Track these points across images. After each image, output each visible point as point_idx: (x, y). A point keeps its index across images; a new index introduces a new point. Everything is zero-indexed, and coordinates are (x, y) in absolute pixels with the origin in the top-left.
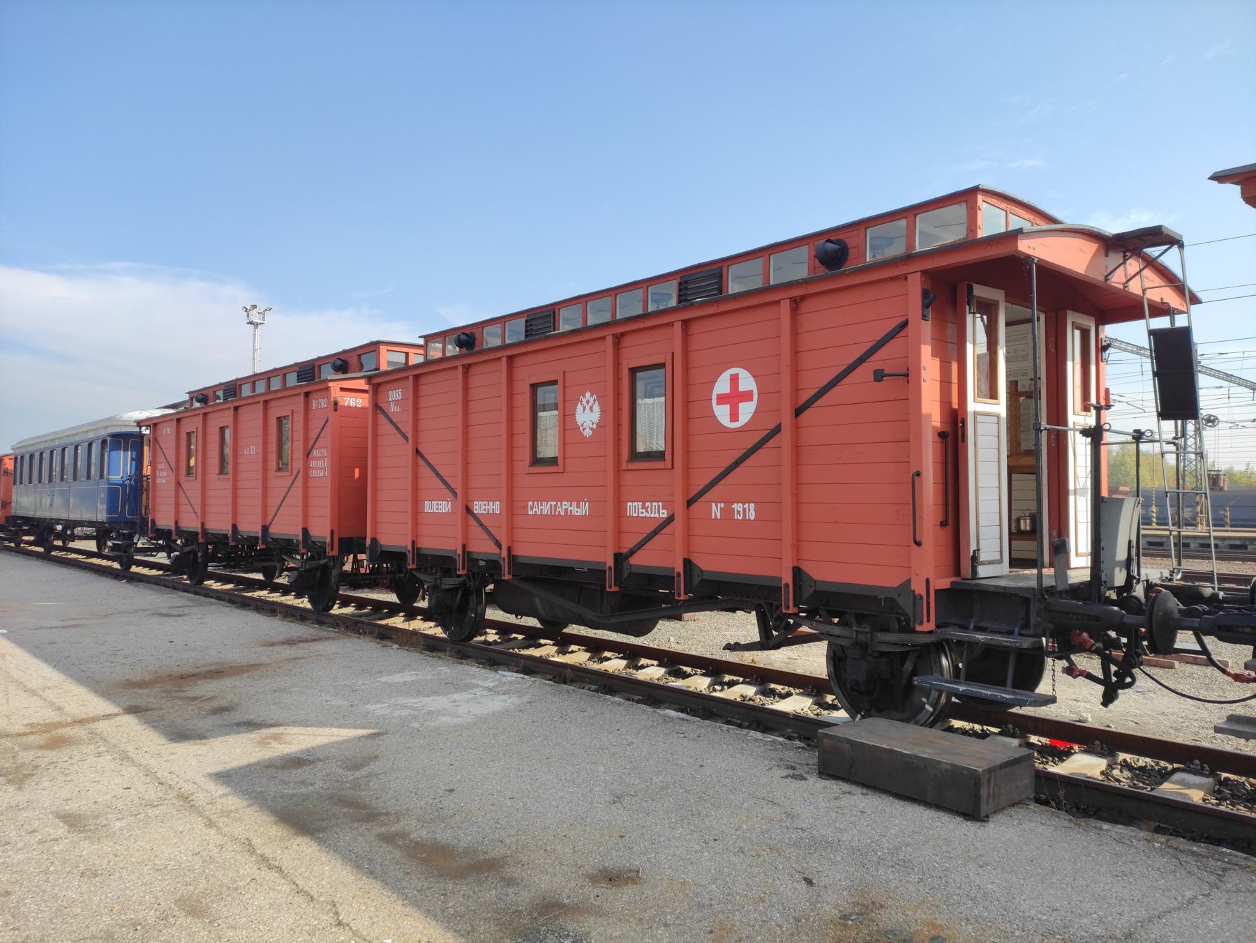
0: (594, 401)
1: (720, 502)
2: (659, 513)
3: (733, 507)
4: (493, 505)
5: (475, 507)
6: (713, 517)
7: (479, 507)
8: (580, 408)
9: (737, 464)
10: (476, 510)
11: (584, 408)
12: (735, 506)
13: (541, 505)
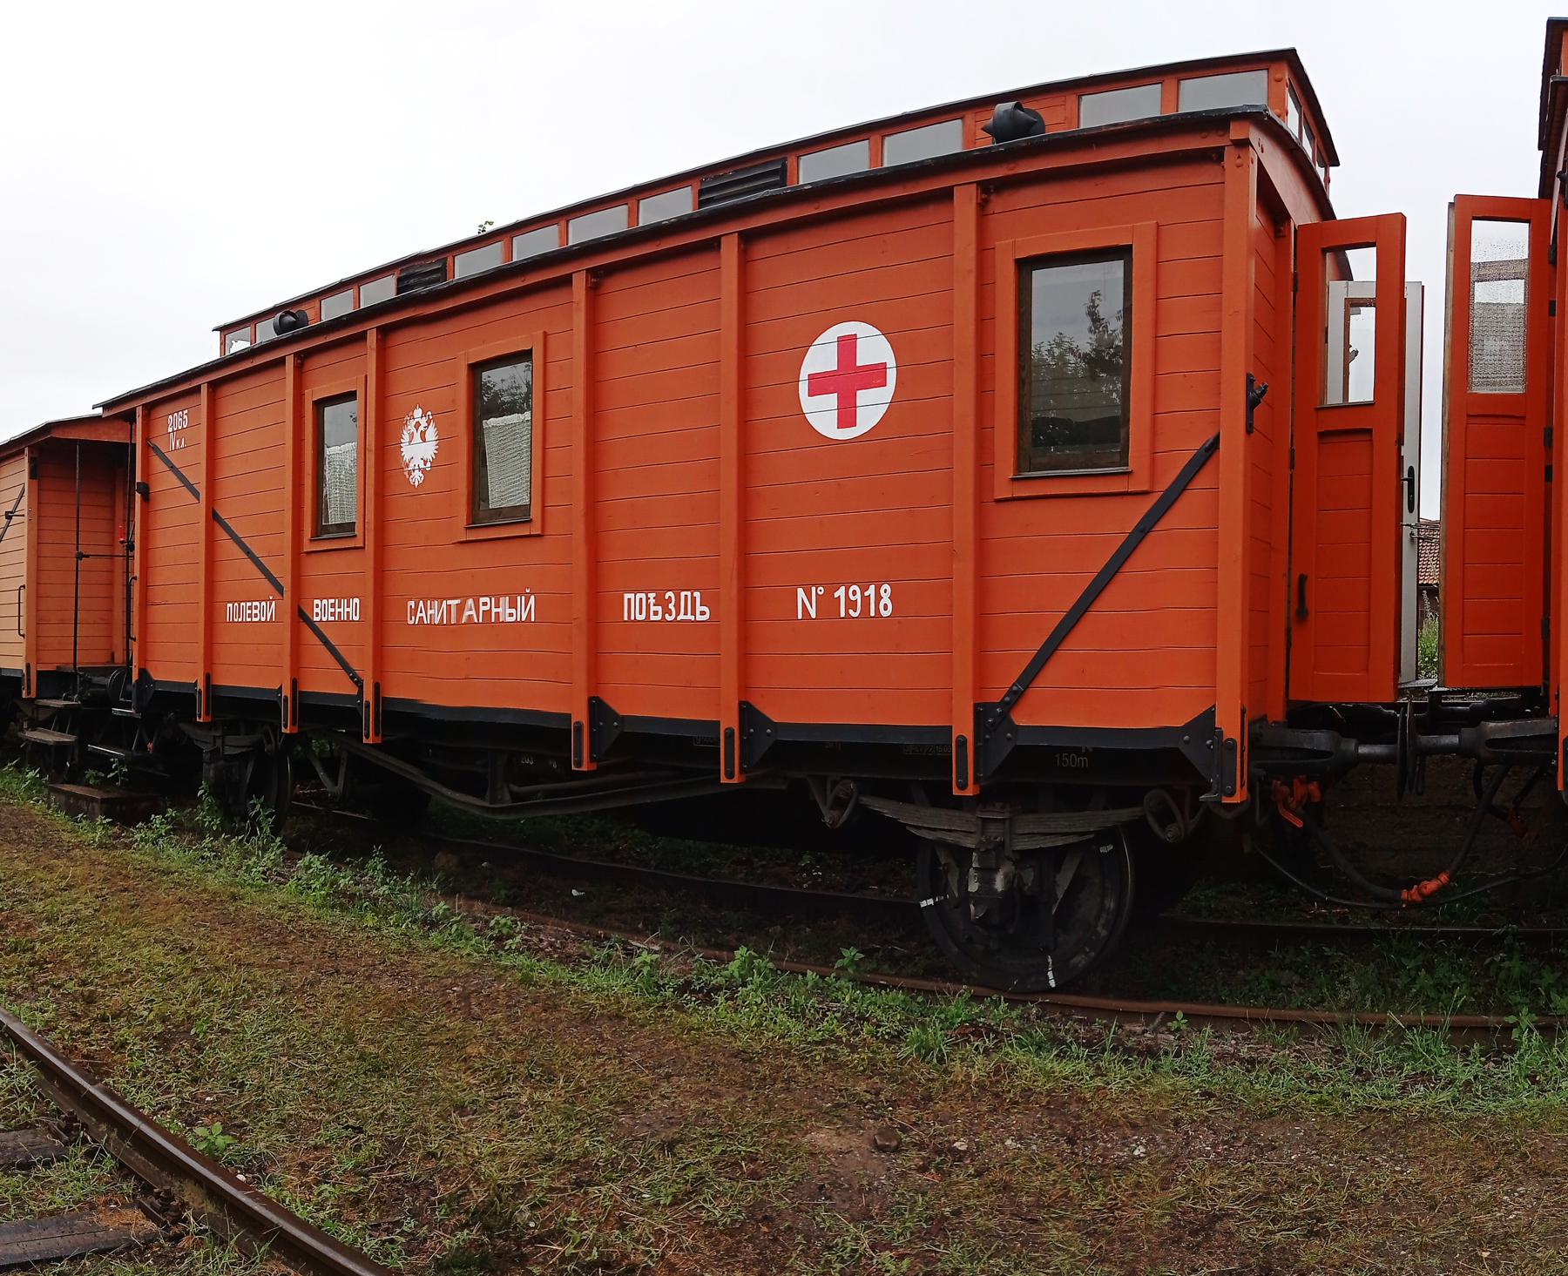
1: (817, 586)
2: (694, 613)
5: (316, 610)
7: (322, 610)
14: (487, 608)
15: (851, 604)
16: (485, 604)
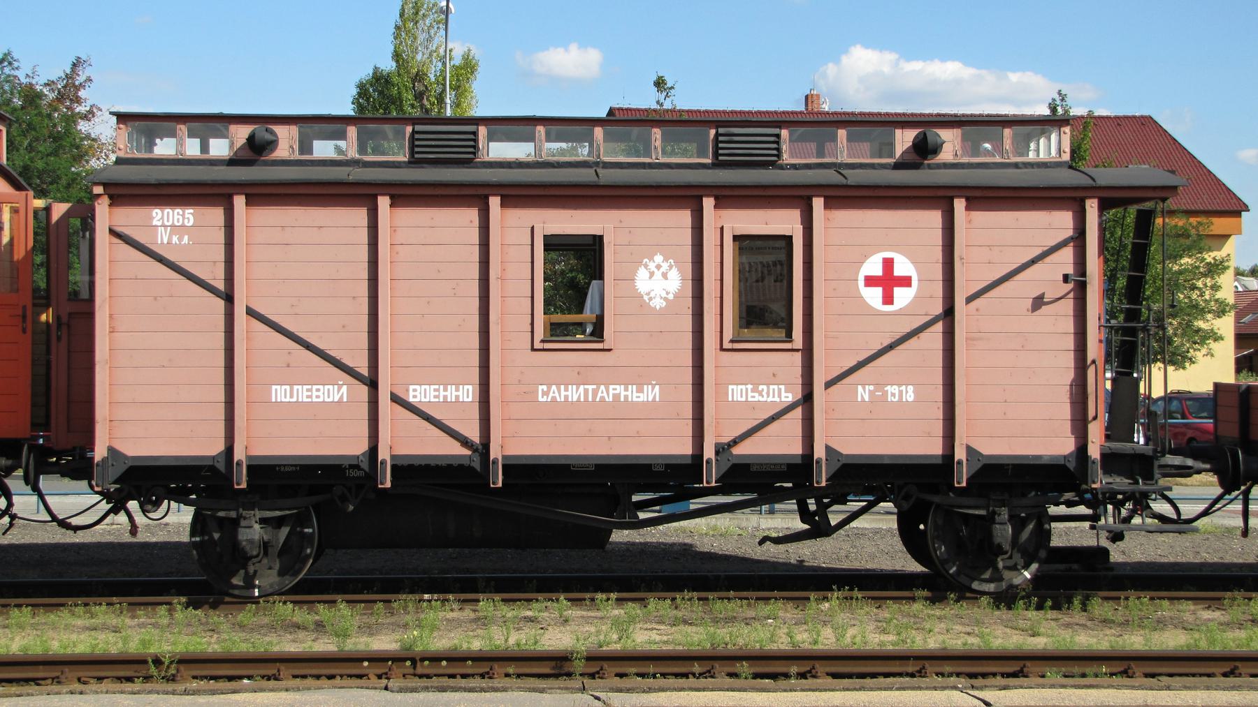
0: (671, 267)
1: (869, 385)
2: (780, 396)
3: (886, 389)
5: (411, 393)
6: (859, 399)
8: (642, 273)
9: (891, 347)
11: (652, 274)
12: (888, 388)
13: (566, 390)
14: (617, 392)
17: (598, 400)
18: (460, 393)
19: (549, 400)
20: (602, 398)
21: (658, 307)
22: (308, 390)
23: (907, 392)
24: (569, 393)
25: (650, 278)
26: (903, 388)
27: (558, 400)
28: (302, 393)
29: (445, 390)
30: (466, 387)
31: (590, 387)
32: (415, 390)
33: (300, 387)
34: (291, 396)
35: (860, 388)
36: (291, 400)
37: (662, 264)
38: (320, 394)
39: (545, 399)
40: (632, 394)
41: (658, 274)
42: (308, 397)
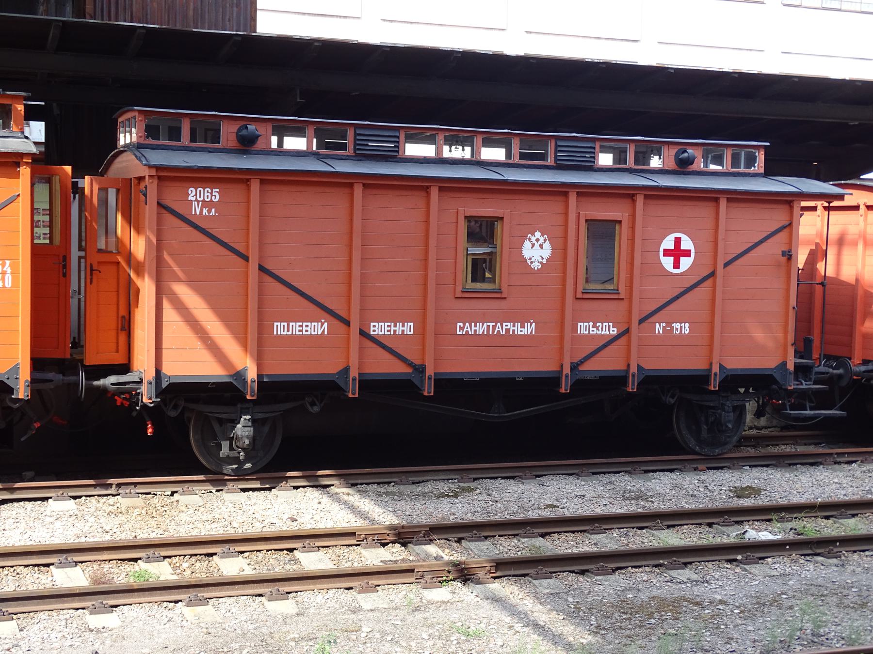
0: (545, 240)
1: (663, 322)
2: (609, 330)
4: (403, 326)
5: (372, 328)
8: (527, 244)
10: (374, 331)
11: (533, 245)
12: (674, 325)
13: (475, 326)
14: (508, 327)
15: (677, 329)
16: (506, 326)
17: (495, 333)
18: (405, 328)
19: (464, 333)
20: (499, 332)
21: (536, 269)
22: (300, 326)
23: (685, 327)
24: (477, 328)
25: (532, 248)
26: (683, 324)
27: (470, 333)
28: (296, 328)
29: (395, 326)
30: (409, 324)
31: (491, 324)
32: (374, 326)
33: (294, 324)
34: (288, 331)
35: (657, 324)
36: (288, 333)
37: (540, 238)
38: (308, 329)
39: (461, 333)
40: (518, 329)
41: (537, 245)
42: (300, 331)
